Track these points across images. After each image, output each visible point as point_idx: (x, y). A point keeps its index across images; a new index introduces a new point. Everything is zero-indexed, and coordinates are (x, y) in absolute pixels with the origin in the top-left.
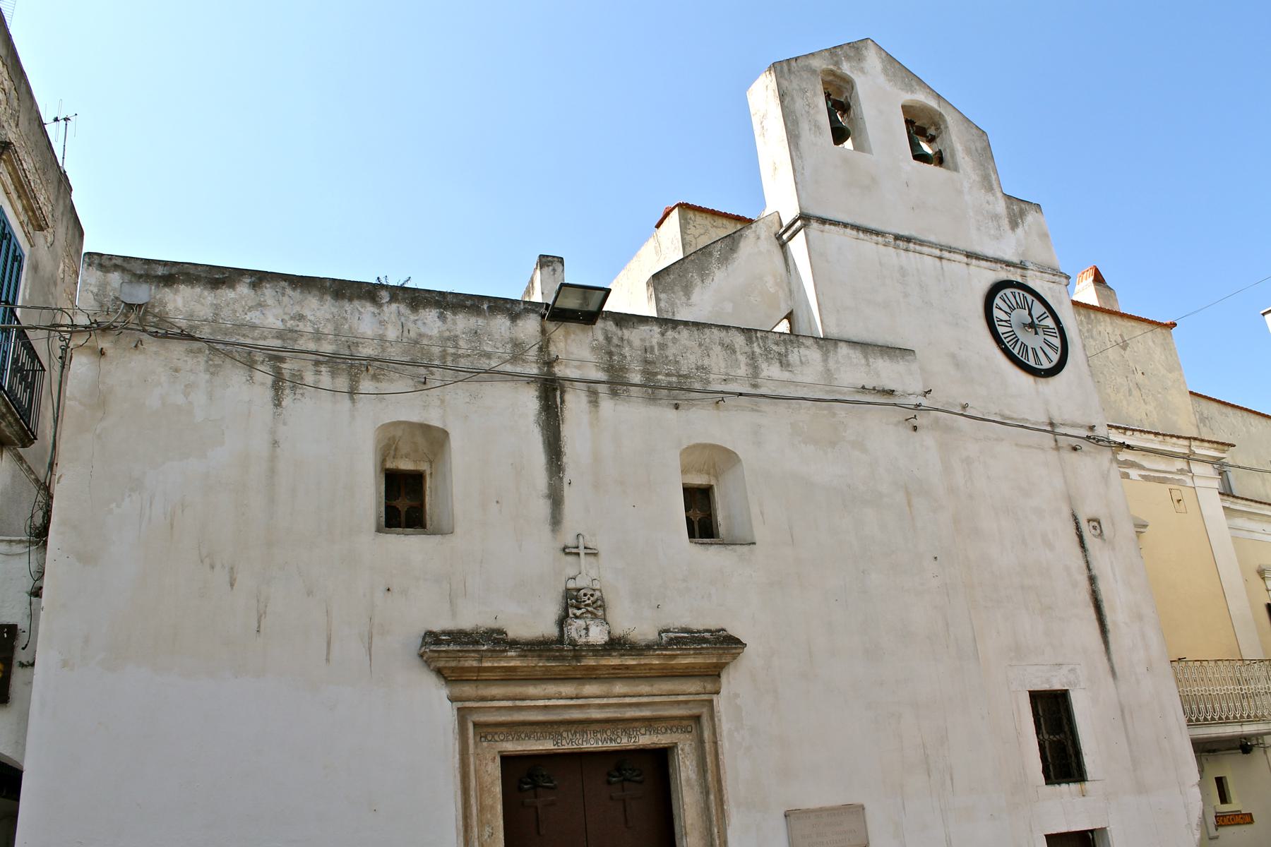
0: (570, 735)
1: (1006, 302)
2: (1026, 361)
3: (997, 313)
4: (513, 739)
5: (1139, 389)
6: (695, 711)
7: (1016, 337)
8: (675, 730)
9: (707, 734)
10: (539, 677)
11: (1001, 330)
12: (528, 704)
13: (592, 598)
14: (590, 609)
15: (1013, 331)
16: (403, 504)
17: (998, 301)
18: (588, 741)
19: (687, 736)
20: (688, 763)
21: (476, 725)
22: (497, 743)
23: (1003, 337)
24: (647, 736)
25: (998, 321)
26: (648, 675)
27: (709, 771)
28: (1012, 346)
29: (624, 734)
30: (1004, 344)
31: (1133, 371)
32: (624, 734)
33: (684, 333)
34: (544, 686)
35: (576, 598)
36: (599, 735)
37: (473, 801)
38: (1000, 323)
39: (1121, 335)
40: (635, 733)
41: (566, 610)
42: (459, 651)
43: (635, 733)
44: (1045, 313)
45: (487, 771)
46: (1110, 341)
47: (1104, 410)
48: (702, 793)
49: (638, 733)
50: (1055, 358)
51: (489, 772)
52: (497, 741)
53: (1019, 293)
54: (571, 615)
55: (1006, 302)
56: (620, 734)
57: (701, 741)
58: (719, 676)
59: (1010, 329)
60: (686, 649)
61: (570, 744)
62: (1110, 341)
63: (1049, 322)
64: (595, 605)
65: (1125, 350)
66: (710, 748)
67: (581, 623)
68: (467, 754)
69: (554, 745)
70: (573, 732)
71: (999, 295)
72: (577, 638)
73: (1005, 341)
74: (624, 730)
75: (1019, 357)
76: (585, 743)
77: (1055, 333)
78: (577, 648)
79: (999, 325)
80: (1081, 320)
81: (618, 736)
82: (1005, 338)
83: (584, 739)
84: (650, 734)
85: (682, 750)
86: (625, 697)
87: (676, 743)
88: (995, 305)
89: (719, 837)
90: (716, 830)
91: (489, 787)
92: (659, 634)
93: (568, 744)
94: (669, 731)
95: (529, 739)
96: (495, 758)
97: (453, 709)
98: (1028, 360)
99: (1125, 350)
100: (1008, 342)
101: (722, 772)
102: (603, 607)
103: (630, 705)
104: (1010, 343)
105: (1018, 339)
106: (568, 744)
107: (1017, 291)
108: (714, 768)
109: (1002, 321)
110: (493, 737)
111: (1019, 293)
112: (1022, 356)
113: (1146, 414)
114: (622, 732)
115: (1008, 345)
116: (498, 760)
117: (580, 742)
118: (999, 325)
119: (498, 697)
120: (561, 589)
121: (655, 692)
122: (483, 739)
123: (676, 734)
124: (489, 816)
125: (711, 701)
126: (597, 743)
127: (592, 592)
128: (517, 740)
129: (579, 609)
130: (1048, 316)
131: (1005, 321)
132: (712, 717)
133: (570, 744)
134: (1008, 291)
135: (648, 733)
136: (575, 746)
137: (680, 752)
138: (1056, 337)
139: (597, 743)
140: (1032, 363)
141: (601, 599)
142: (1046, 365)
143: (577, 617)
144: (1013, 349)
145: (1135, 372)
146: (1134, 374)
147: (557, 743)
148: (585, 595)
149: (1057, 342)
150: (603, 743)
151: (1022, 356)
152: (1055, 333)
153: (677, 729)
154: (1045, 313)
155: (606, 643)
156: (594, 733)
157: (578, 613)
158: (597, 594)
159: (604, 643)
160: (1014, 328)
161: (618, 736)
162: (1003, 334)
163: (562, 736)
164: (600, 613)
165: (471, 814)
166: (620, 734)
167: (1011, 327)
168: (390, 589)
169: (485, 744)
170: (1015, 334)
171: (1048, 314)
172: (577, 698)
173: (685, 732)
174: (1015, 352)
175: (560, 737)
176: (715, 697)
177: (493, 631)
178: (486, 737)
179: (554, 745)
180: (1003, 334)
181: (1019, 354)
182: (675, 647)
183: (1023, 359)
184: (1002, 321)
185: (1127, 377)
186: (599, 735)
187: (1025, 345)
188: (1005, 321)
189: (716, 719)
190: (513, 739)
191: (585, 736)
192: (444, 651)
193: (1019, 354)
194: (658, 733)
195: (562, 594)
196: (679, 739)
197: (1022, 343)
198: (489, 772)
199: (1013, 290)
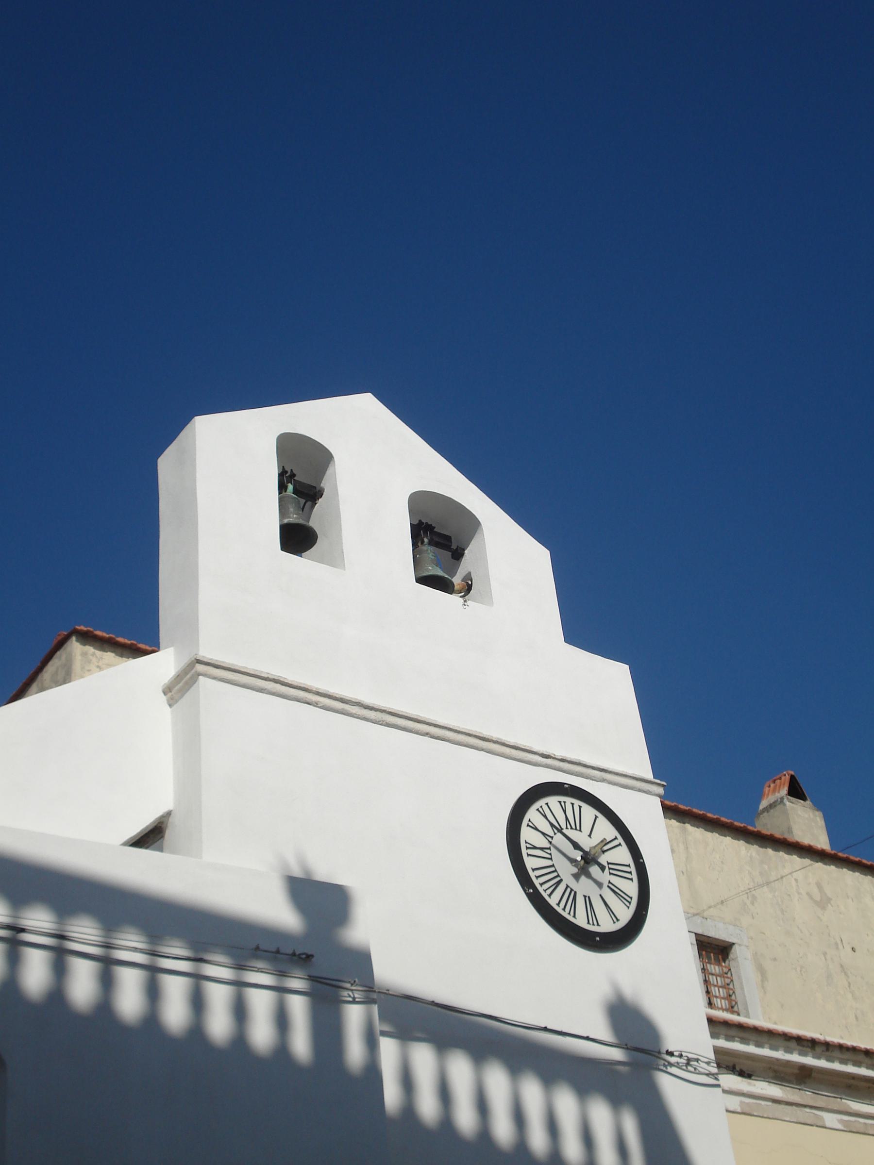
1: (545, 817)
2: (570, 918)
3: (527, 835)
5: (846, 974)
7: (558, 876)
11: (530, 863)
15: (553, 866)
16: (433, 1004)
23: (532, 875)
25: (527, 848)
28: (549, 892)
30: (533, 885)
31: (836, 944)
33: (798, 868)
38: (531, 852)
39: (819, 886)
44: (616, 838)
46: (799, 893)
47: (782, 1006)
50: (625, 914)
55: (545, 817)
59: (549, 863)
62: (799, 893)
63: (622, 855)
65: (824, 908)
71: (537, 805)
73: (537, 882)
75: (559, 910)
77: (630, 873)
79: (528, 855)
80: (751, 857)
82: (537, 877)
88: (525, 821)
98: (574, 916)
99: (824, 908)
100: (541, 884)
104: (546, 886)
105: (561, 880)
107: (569, 800)
109: (535, 848)
111: (573, 804)
112: (564, 909)
113: (857, 1018)
115: (541, 889)
118: (528, 855)
130: (620, 844)
131: (542, 849)
134: (553, 801)
138: (631, 879)
140: (581, 920)
142: (607, 925)
144: (550, 895)
145: (840, 947)
146: (837, 948)
149: (631, 888)
151: (564, 909)
152: (630, 873)
154: (616, 838)
160: (555, 862)
162: (534, 870)
167: (551, 859)
170: (556, 871)
171: (620, 840)
174: (553, 901)
180: (534, 870)
181: (558, 904)
183: (565, 914)
184: (535, 848)
185: (825, 954)
187: (572, 890)
188: (542, 849)
193: (558, 904)
197: (567, 886)
199: (562, 799)
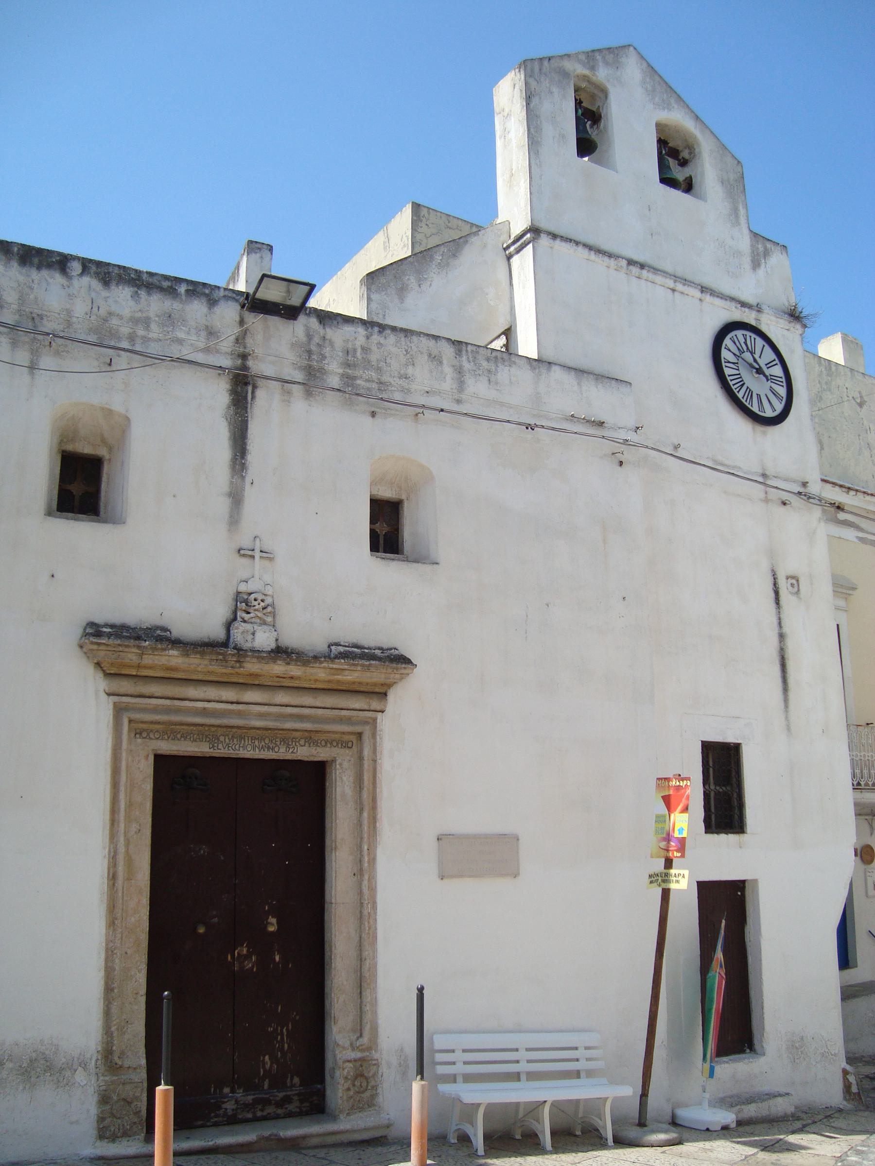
0: (227, 740)
1: (735, 343)
2: (750, 406)
3: (725, 354)
4: (168, 738)
5: (870, 449)
6: (358, 729)
8: (335, 744)
9: (366, 752)
10: (200, 677)
11: (727, 371)
12: (186, 705)
13: (262, 604)
14: (259, 614)
15: (739, 374)
17: (727, 341)
18: (245, 748)
19: (347, 752)
20: (345, 778)
21: (130, 721)
22: (152, 741)
23: (729, 378)
24: (305, 748)
25: (725, 362)
26: (313, 686)
27: (365, 789)
28: (738, 390)
29: (282, 743)
32: (282, 743)
34: (205, 689)
35: (246, 602)
36: (256, 743)
37: (122, 796)
38: (728, 364)
40: (294, 744)
41: (235, 613)
42: (119, 645)
43: (294, 744)
44: (774, 360)
45: (139, 768)
48: (356, 809)
49: (297, 744)
50: (779, 407)
51: (141, 769)
52: (151, 739)
53: (750, 337)
54: (239, 618)
55: (735, 343)
56: (278, 743)
57: (361, 758)
58: (385, 694)
59: (737, 372)
60: (354, 665)
61: (227, 749)
63: (777, 371)
64: (265, 611)
66: (369, 766)
67: (248, 626)
69: (210, 748)
70: (230, 737)
72: (242, 642)
74: (284, 740)
75: (744, 401)
76: (241, 749)
77: (782, 382)
78: (241, 653)
79: (726, 367)
81: (277, 745)
82: (731, 380)
83: (241, 745)
84: (310, 746)
85: (341, 764)
86: (287, 706)
87: (335, 758)
89: (369, 854)
90: (366, 847)
91: (139, 783)
92: (329, 646)
93: (224, 749)
94: (329, 745)
95: (185, 740)
96: (148, 756)
97: (109, 703)
98: (752, 406)
100: (734, 385)
101: (378, 790)
102: (274, 614)
103: (292, 717)
105: (744, 384)
106: (224, 749)
107: (748, 334)
108: (371, 786)
109: (729, 362)
110: (148, 734)
111: (750, 337)
112: (746, 401)
114: (281, 742)
116: (151, 759)
117: (237, 747)
118: (726, 367)
119: (157, 694)
120: (232, 591)
121: (318, 704)
122: (138, 736)
123: (336, 748)
124: (137, 813)
125: (375, 720)
126: (254, 750)
127: (263, 597)
128: (172, 739)
129: (248, 613)
130: (776, 364)
131: (734, 363)
132: (374, 735)
133: (227, 749)
135: (307, 744)
136: (232, 751)
137: (338, 766)
138: (783, 386)
139: (254, 750)
140: (755, 409)
141: (272, 605)
142: (769, 413)
143: (244, 621)
144: (738, 392)
145: (869, 432)
146: (867, 433)
147: (213, 746)
148: (255, 600)
149: (782, 391)
150: (260, 751)
151: (746, 401)
152: (782, 382)
153: (337, 744)
154: (774, 360)
155: (272, 651)
156: (252, 740)
157: (247, 617)
158: (269, 600)
159: (270, 650)
161: (277, 745)
162: (729, 376)
163: (218, 739)
164: (269, 619)
165: (119, 809)
166: (278, 743)
167: (738, 370)
168: (55, 576)
169: (139, 741)
171: (777, 361)
172: (238, 703)
173: (345, 747)
174: (740, 395)
175: (216, 741)
176: (379, 715)
177: (158, 628)
178: (141, 734)
179: (210, 748)
180: (729, 376)
181: (743, 398)
182: (343, 661)
183: (747, 404)
184: (729, 362)
185: (859, 435)
186: (256, 743)
187: (750, 390)
188: (734, 363)
189: (378, 737)
190: (168, 738)
191: (243, 742)
192: (104, 644)
193: (743, 398)
194: (317, 745)
195: (233, 597)
196: (338, 754)
197: (748, 388)
198: (141, 769)
199: (745, 332)
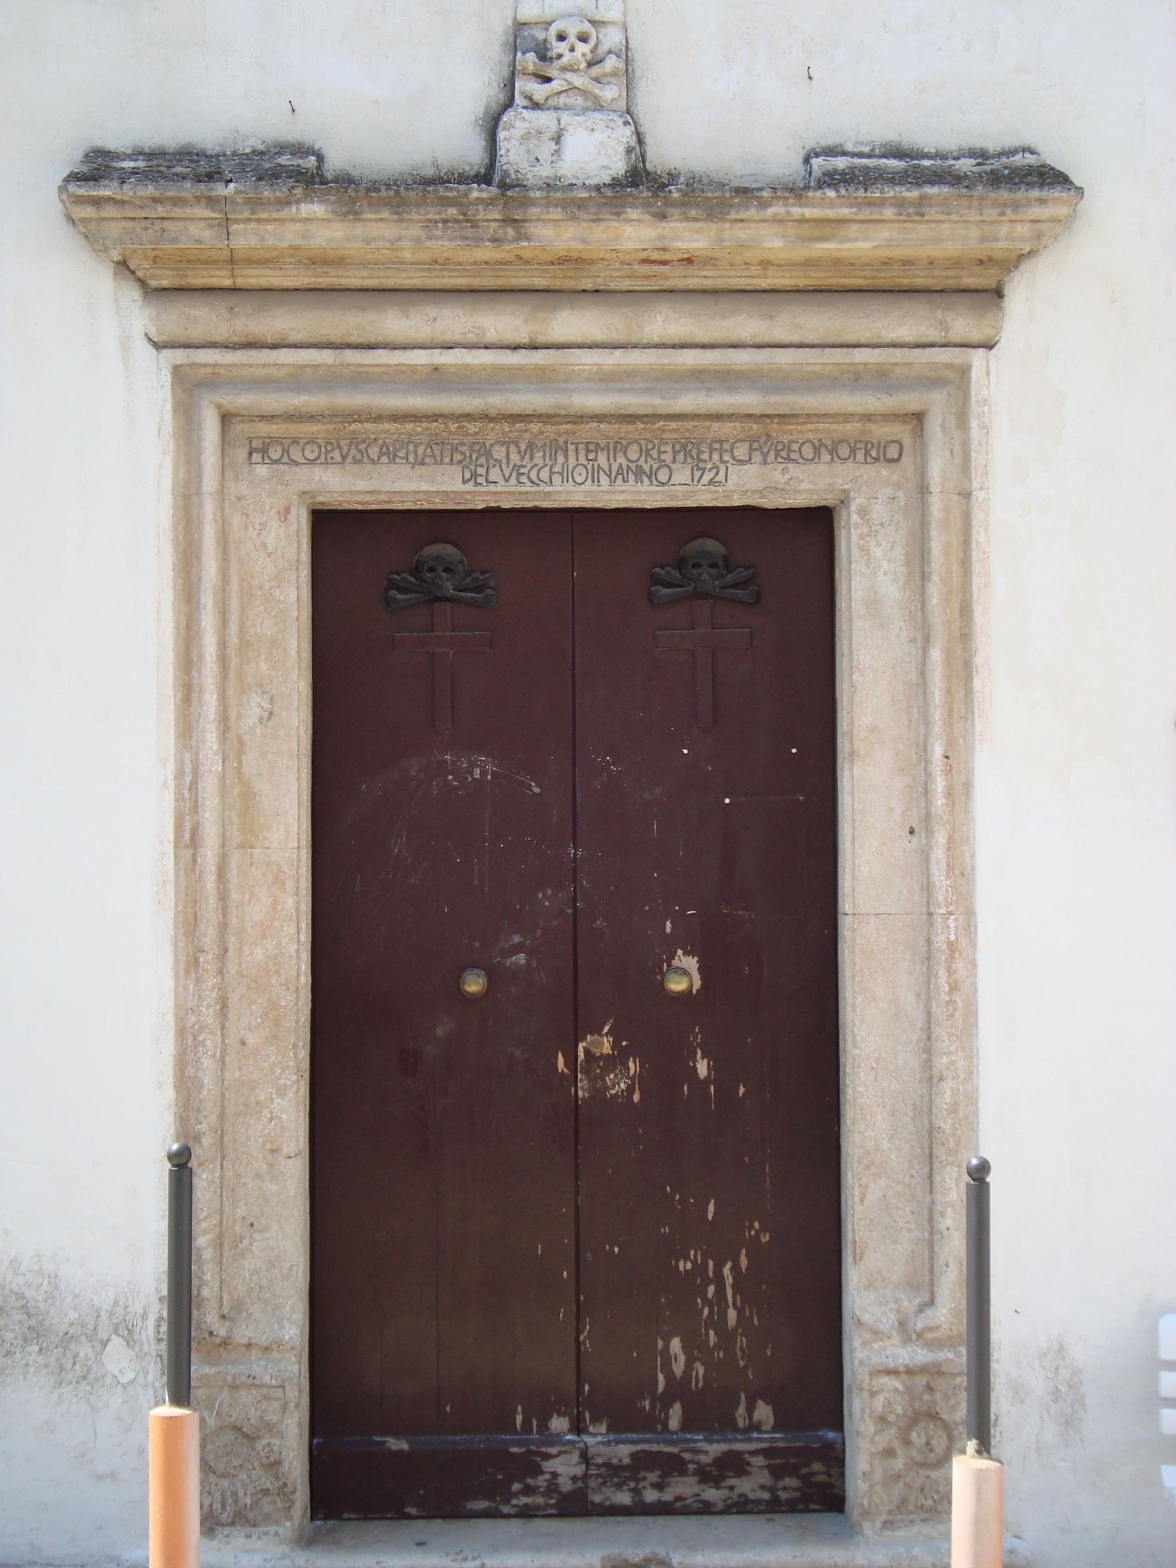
0: (515, 457)
4: (344, 458)
6: (909, 401)
8: (844, 451)
9: (936, 470)
14: (578, 81)
18: (567, 475)
19: (884, 473)
20: (877, 552)
22: (296, 469)
24: (752, 469)
26: (764, 284)
27: (935, 578)
29: (681, 457)
32: (681, 457)
35: (543, 55)
36: (602, 460)
40: (716, 457)
41: (510, 85)
43: (716, 457)
45: (264, 545)
48: (913, 641)
49: (727, 457)
51: (270, 549)
52: (295, 463)
54: (519, 100)
56: (668, 457)
57: (923, 489)
60: (871, 203)
61: (513, 480)
64: (595, 71)
66: (946, 510)
68: (199, 493)
69: (464, 482)
70: (523, 447)
74: (684, 447)
76: (557, 479)
81: (663, 464)
83: (557, 469)
84: (765, 463)
85: (863, 512)
86: (683, 346)
87: (846, 492)
93: (507, 480)
94: (826, 457)
95: (392, 461)
96: (287, 510)
101: (976, 582)
102: (628, 76)
103: (699, 377)
106: (507, 480)
108: (956, 568)
110: (286, 451)
114: (675, 454)
117: (545, 474)
120: (500, 25)
121: (780, 335)
123: (849, 465)
126: (596, 480)
128: (355, 461)
129: (548, 80)
133: (513, 480)
135: (757, 457)
136: (528, 487)
137: (855, 517)
139: (596, 480)
141: (626, 53)
147: (474, 475)
150: (612, 482)
153: (853, 451)
156: (588, 451)
158: (612, 38)
161: (663, 464)
163: (488, 455)
164: (609, 93)
166: (668, 457)
169: (262, 470)
172: (535, 347)
175: (482, 460)
178: (264, 451)
179: (464, 482)
186: (602, 460)
190: (344, 458)
191: (561, 459)
194: (788, 459)
195: (503, 39)
196: (854, 480)
198: (270, 549)
